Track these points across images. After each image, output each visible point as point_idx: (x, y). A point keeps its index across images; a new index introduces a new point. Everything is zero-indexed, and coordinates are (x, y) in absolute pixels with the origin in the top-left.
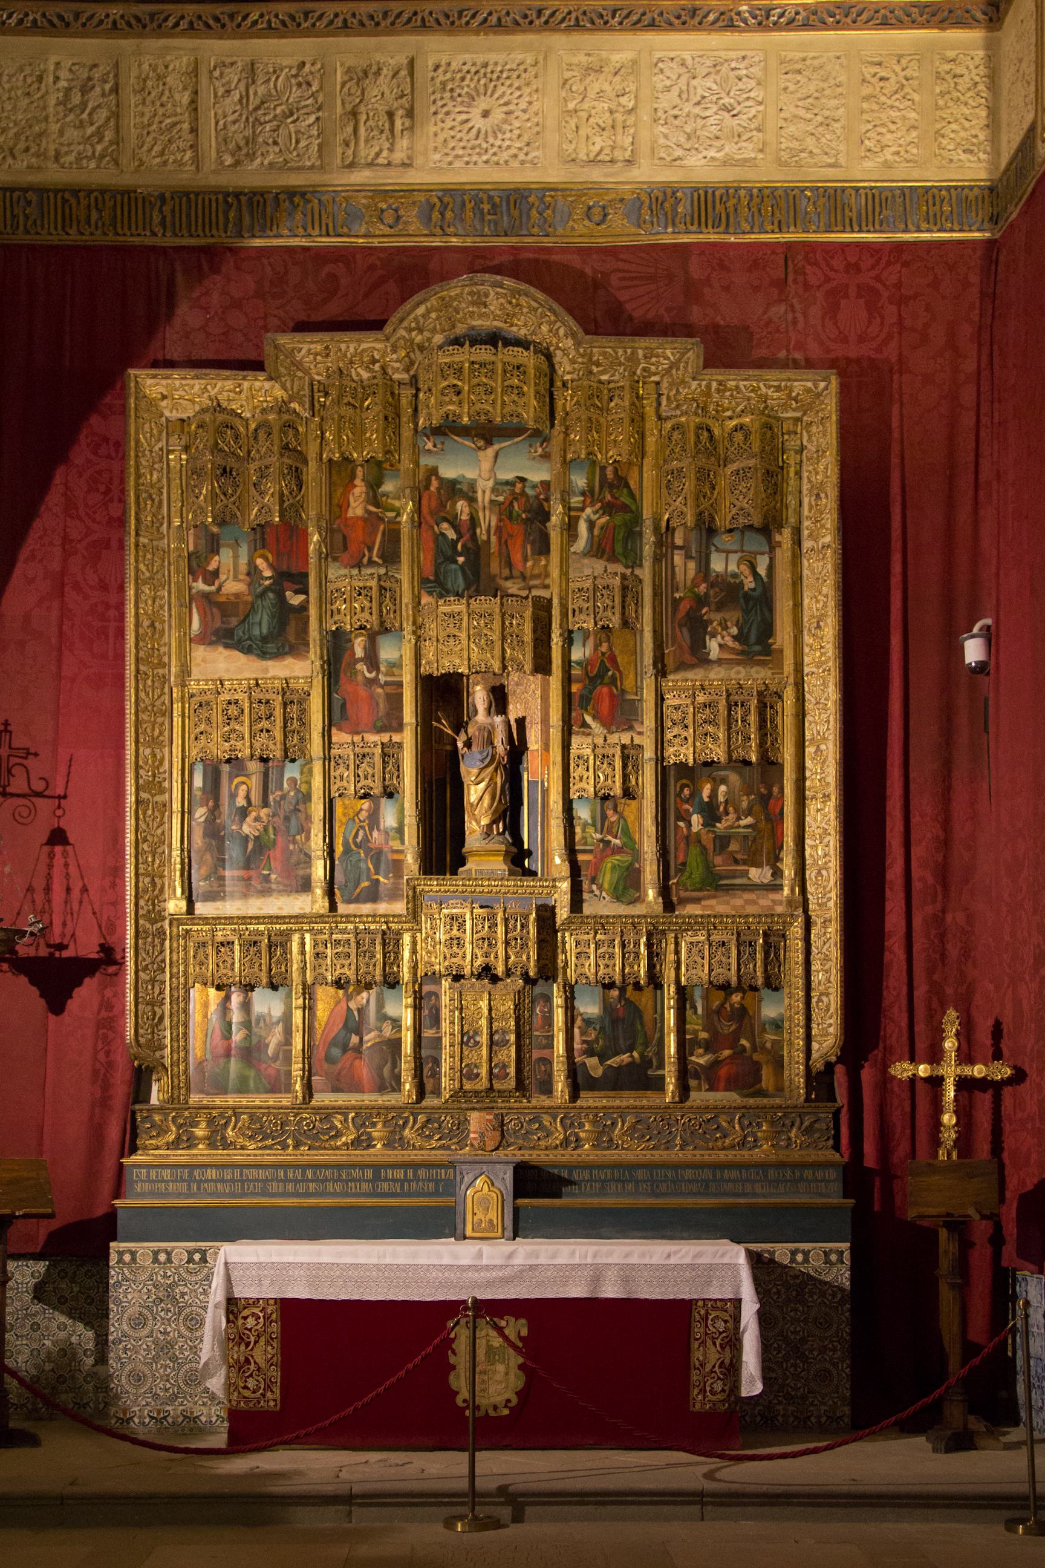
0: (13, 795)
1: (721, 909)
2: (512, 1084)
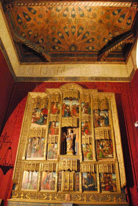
0: (5, 142)
1: (105, 161)
2: (73, 189)
